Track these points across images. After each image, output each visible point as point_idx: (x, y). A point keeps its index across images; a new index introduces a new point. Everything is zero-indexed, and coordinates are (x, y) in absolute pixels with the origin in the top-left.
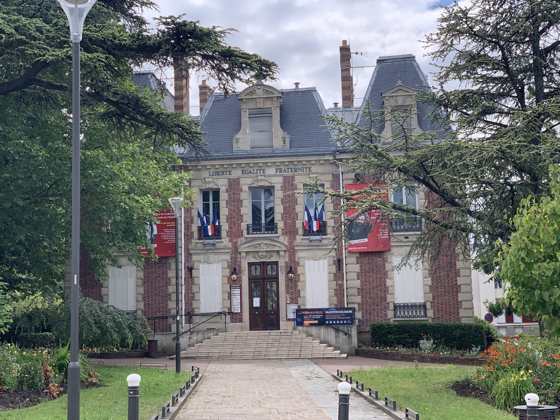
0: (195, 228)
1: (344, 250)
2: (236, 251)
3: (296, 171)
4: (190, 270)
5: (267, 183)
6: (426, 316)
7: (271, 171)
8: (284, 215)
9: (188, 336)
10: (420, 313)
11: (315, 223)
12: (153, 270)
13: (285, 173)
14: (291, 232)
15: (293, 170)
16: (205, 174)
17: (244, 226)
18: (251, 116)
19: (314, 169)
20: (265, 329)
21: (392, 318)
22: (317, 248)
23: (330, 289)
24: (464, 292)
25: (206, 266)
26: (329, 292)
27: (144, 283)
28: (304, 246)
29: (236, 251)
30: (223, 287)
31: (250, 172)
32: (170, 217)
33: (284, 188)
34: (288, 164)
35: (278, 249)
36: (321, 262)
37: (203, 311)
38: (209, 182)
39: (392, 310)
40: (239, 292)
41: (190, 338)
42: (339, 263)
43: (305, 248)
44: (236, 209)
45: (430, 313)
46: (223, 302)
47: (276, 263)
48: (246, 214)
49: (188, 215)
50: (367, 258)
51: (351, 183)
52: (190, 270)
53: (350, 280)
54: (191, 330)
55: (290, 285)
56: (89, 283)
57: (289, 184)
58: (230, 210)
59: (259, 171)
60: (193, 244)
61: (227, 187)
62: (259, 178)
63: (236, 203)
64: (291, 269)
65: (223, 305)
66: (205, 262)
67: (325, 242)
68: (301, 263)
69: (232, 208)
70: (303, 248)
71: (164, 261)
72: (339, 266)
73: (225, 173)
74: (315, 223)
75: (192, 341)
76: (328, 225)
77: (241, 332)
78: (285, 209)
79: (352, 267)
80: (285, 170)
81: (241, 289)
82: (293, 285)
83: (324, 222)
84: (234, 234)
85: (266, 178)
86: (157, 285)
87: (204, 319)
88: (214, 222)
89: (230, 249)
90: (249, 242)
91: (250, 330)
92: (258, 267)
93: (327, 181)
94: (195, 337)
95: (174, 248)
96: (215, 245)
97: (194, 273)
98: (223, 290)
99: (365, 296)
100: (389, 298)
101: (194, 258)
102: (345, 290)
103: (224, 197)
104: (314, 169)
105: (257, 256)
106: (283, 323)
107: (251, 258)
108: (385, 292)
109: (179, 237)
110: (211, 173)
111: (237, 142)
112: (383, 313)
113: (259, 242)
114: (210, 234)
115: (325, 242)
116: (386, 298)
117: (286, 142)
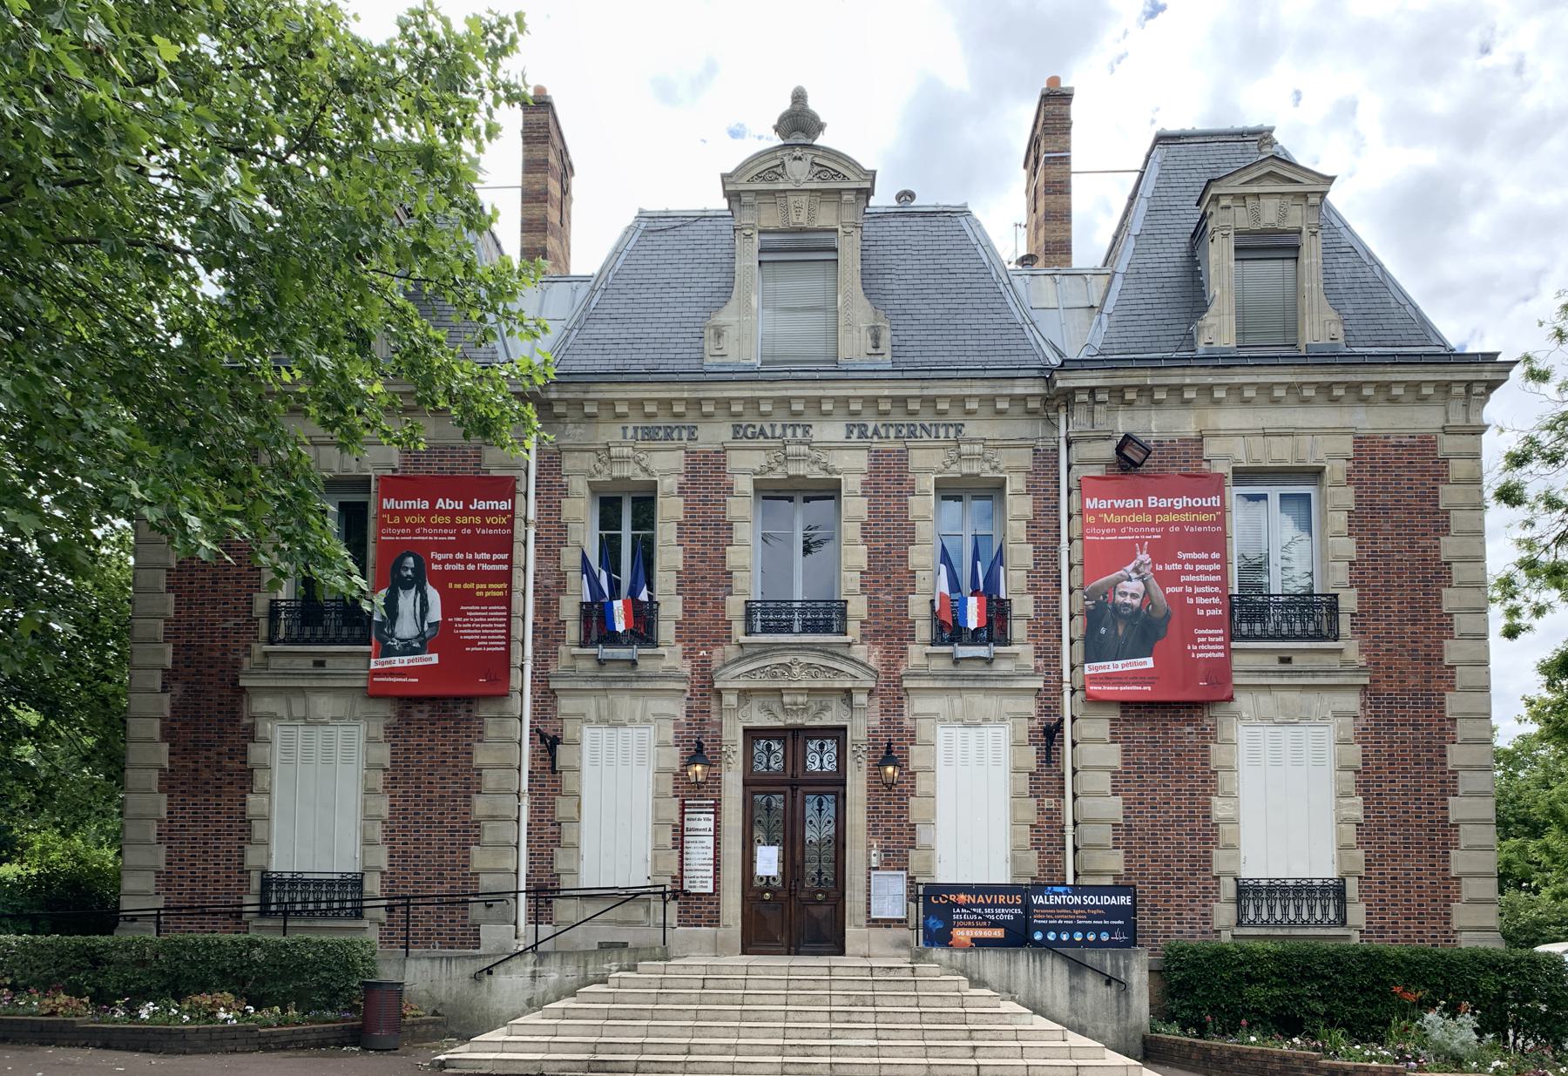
0: (569, 608)
1: (1067, 695)
2: (705, 689)
3: (912, 434)
4: (549, 743)
5: (816, 468)
6: (1344, 923)
7: (830, 431)
8: (869, 578)
9: (529, 969)
10: (1325, 914)
11: (973, 602)
12: (424, 741)
13: (875, 439)
14: (890, 631)
15: (905, 431)
16: (609, 433)
17: (734, 607)
18: (766, 257)
19: (971, 429)
20: (794, 948)
21: (1228, 928)
22: (978, 684)
23: (1015, 822)
24: (1469, 848)
25: (604, 732)
26: (1014, 834)
27: (392, 782)
28: (934, 677)
29: (705, 689)
30: (656, 807)
31: (762, 432)
32: (485, 567)
33: (872, 488)
34: (888, 407)
35: (848, 685)
36: (988, 732)
37: (589, 877)
38: (623, 460)
39: (1228, 901)
40: (711, 824)
41: (534, 976)
42: (1050, 736)
43: (939, 684)
44: (711, 553)
45: (1357, 914)
46: (655, 858)
47: (838, 733)
48: (744, 569)
49: (551, 565)
50: (1146, 726)
51: (1098, 474)
52: (549, 743)
53: (1086, 794)
54: (541, 948)
55: (883, 806)
56: (206, 775)
57: (889, 479)
58: (690, 555)
59: (789, 432)
60: (564, 660)
61: (682, 479)
62: (790, 449)
63: (709, 533)
64: (890, 751)
65: (655, 865)
66: (601, 721)
67: (1003, 667)
68: (922, 734)
69: (698, 547)
70: (931, 684)
71: (462, 712)
72: (1048, 749)
73: (675, 434)
74: (973, 602)
75: (541, 987)
76: (1015, 611)
77: (711, 957)
78: (873, 555)
79: (1095, 750)
80: (876, 432)
82: (893, 808)
83: (1000, 601)
84: (703, 631)
85: (814, 454)
86: (437, 792)
87: (591, 909)
88: (634, 592)
89: (685, 679)
90: (752, 657)
91: (744, 952)
92: (775, 746)
93: (1017, 470)
94: (553, 974)
95: (499, 666)
96: (634, 663)
97: (564, 755)
98: (656, 817)
99: (1136, 852)
100: (1220, 861)
101: (566, 705)
102: (1069, 829)
103: (670, 509)
104: (971, 429)
105: (775, 707)
106: (854, 933)
107: (755, 711)
108: (1205, 839)
109: (516, 632)
110: (630, 433)
111: (719, 335)
112: (1199, 909)
113: (787, 660)
114: (620, 626)
115: (1003, 667)
116: (1208, 861)
117: (881, 343)
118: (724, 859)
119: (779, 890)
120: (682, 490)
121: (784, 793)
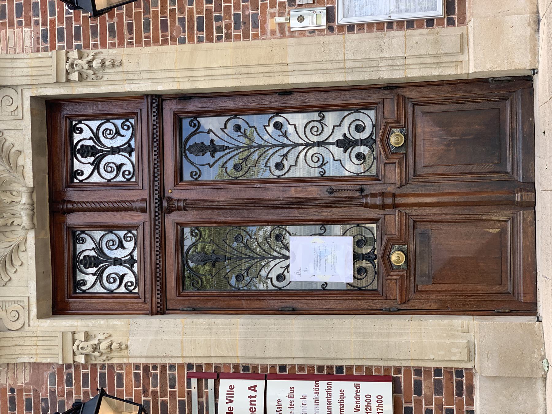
40: (242, 386)
81: (219, 374)
91: (530, 309)
106: (480, 56)
118: (317, 357)
119: (383, 231)
121: (179, 228)
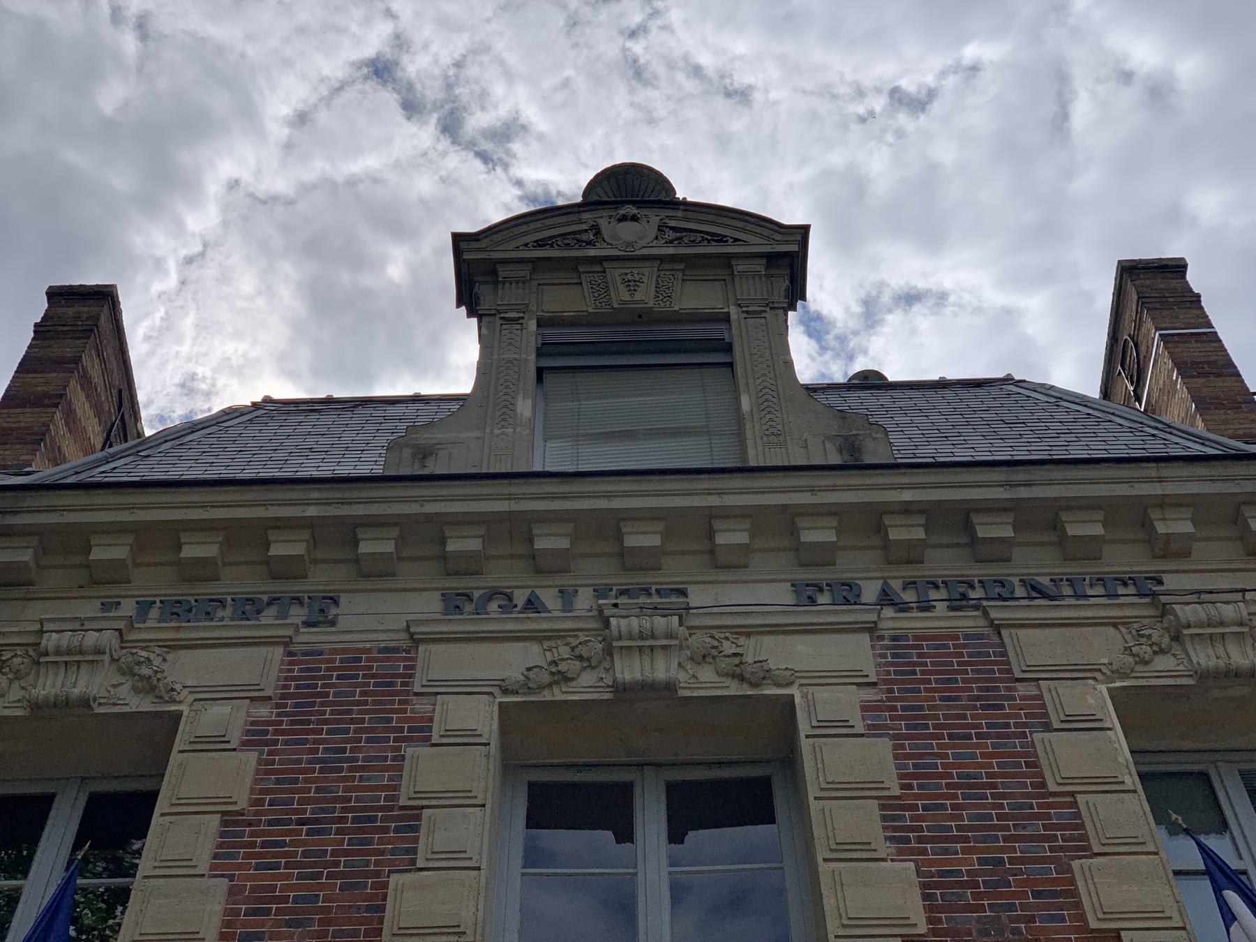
5: (707, 674)
38: (74, 659)
61: (264, 712)
80: (886, 598)
120: (255, 737)
